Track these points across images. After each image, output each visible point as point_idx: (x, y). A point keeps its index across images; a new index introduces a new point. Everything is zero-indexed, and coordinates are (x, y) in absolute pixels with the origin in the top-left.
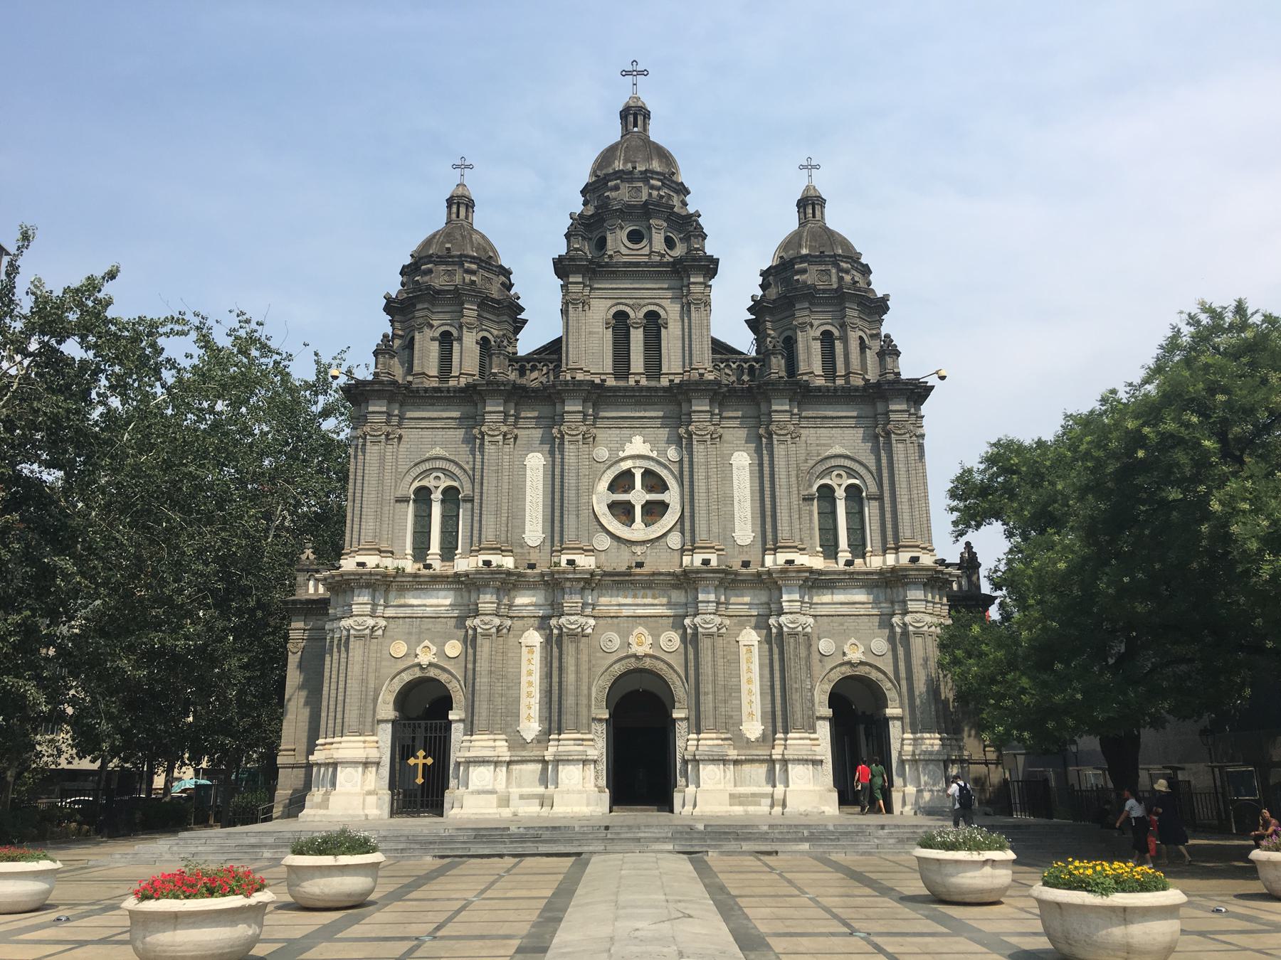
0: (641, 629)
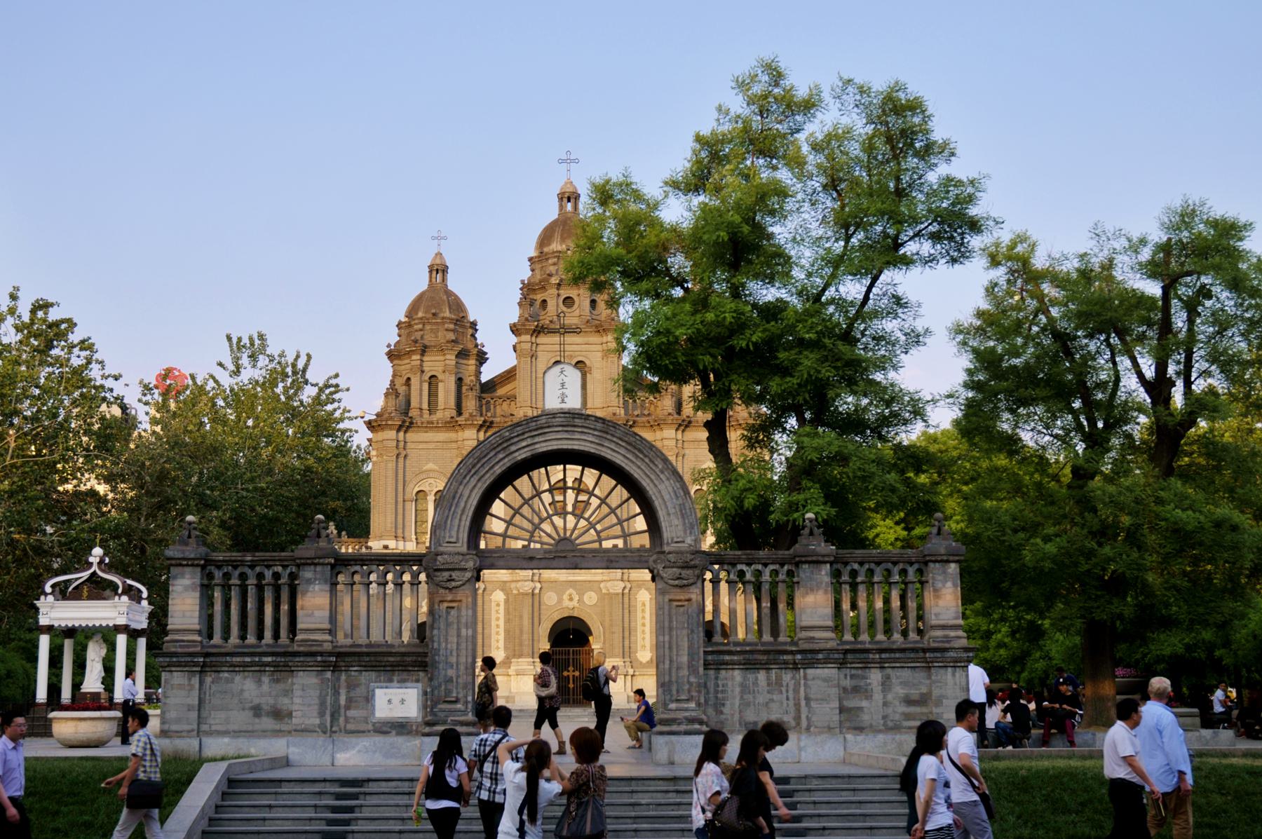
0: (571, 591)
